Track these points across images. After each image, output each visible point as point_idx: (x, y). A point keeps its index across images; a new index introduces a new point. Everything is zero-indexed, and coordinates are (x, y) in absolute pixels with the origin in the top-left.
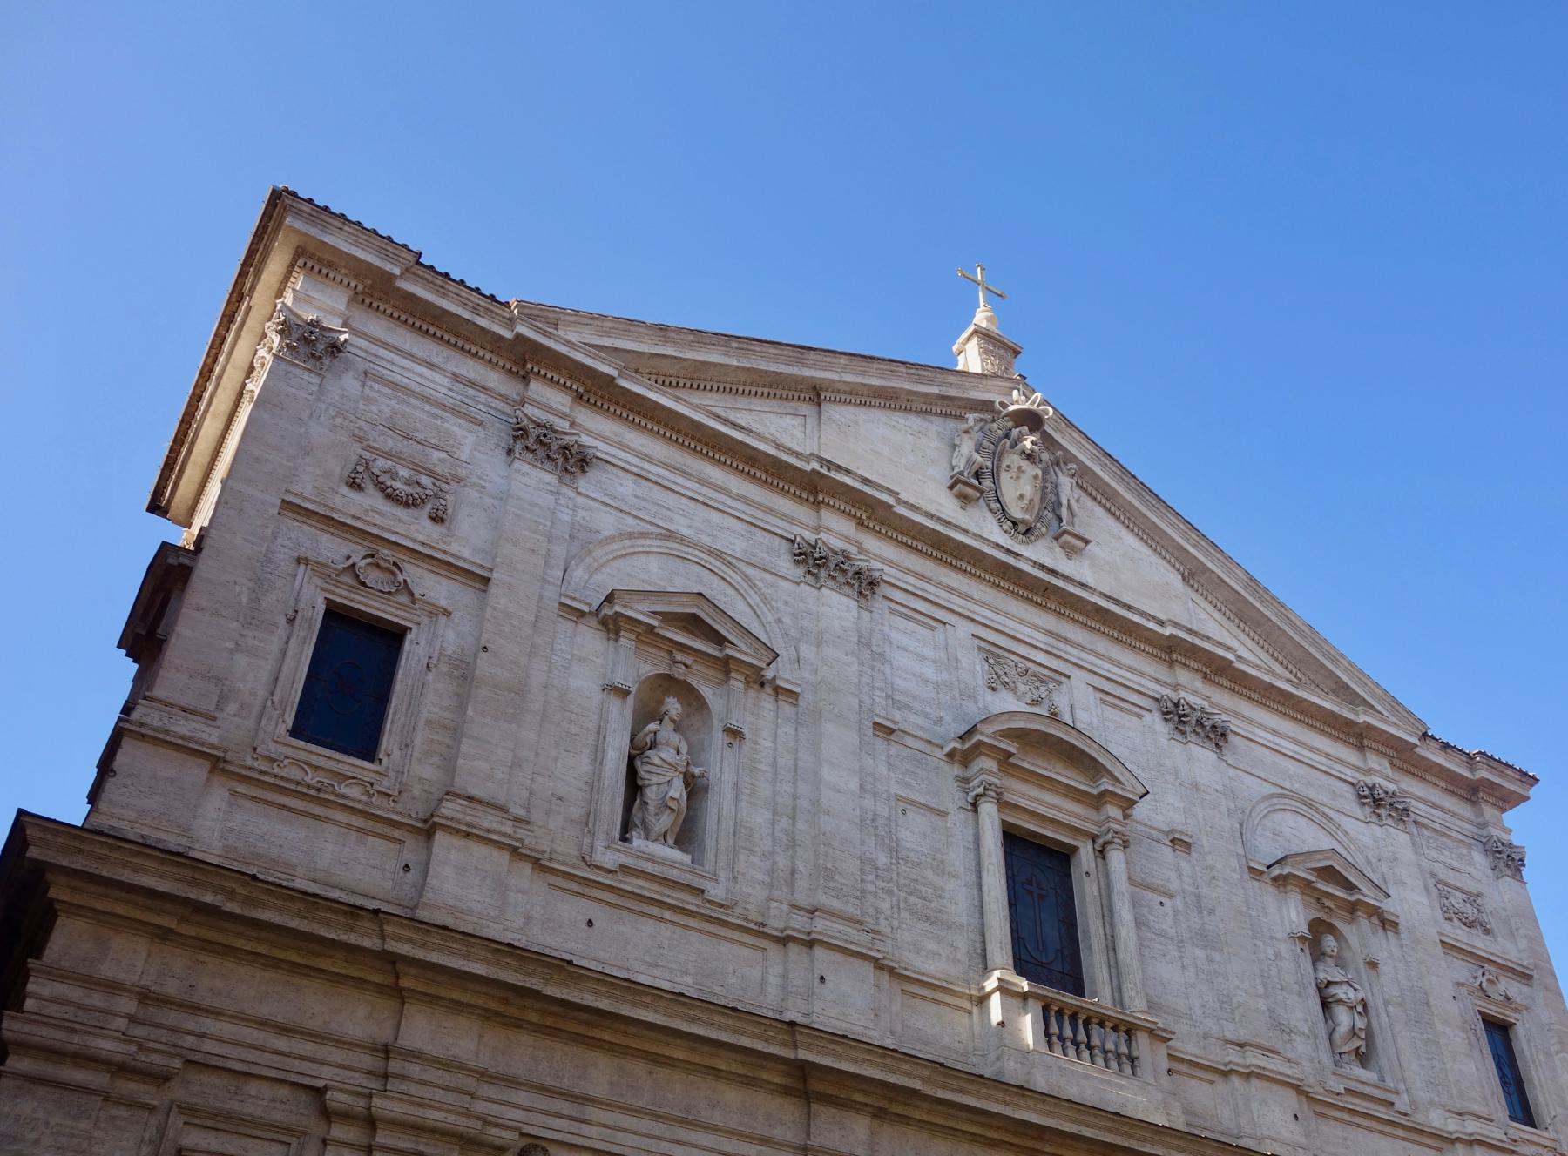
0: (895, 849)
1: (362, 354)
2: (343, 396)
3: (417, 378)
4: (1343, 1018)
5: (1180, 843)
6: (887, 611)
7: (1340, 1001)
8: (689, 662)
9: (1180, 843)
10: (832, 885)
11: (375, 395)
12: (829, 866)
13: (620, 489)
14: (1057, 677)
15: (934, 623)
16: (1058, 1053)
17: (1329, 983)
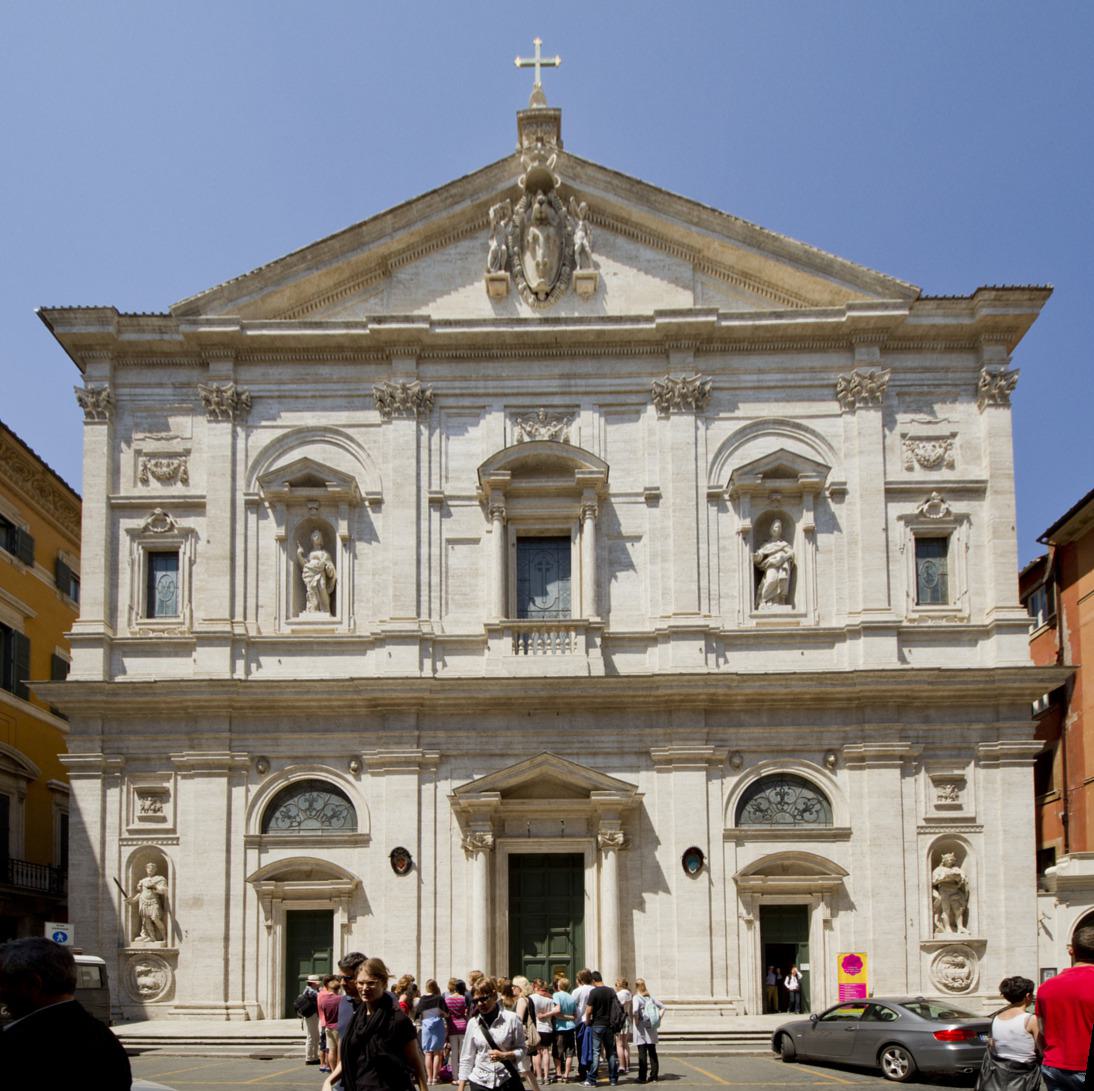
0: (444, 573)
1: (128, 398)
2: (126, 430)
3: (157, 398)
4: (771, 576)
5: (653, 498)
6: (444, 418)
7: (772, 566)
8: (315, 506)
9: (653, 498)
10: (399, 603)
11: (138, 420)
12: (398, 593)
13: (271, 412)
14: (571, 410)
15: (478, 411)
16: (521, 653)
17: (766, 556)
